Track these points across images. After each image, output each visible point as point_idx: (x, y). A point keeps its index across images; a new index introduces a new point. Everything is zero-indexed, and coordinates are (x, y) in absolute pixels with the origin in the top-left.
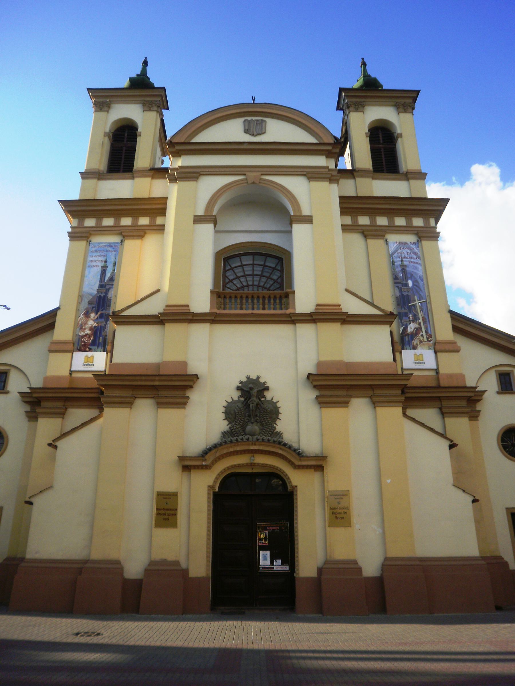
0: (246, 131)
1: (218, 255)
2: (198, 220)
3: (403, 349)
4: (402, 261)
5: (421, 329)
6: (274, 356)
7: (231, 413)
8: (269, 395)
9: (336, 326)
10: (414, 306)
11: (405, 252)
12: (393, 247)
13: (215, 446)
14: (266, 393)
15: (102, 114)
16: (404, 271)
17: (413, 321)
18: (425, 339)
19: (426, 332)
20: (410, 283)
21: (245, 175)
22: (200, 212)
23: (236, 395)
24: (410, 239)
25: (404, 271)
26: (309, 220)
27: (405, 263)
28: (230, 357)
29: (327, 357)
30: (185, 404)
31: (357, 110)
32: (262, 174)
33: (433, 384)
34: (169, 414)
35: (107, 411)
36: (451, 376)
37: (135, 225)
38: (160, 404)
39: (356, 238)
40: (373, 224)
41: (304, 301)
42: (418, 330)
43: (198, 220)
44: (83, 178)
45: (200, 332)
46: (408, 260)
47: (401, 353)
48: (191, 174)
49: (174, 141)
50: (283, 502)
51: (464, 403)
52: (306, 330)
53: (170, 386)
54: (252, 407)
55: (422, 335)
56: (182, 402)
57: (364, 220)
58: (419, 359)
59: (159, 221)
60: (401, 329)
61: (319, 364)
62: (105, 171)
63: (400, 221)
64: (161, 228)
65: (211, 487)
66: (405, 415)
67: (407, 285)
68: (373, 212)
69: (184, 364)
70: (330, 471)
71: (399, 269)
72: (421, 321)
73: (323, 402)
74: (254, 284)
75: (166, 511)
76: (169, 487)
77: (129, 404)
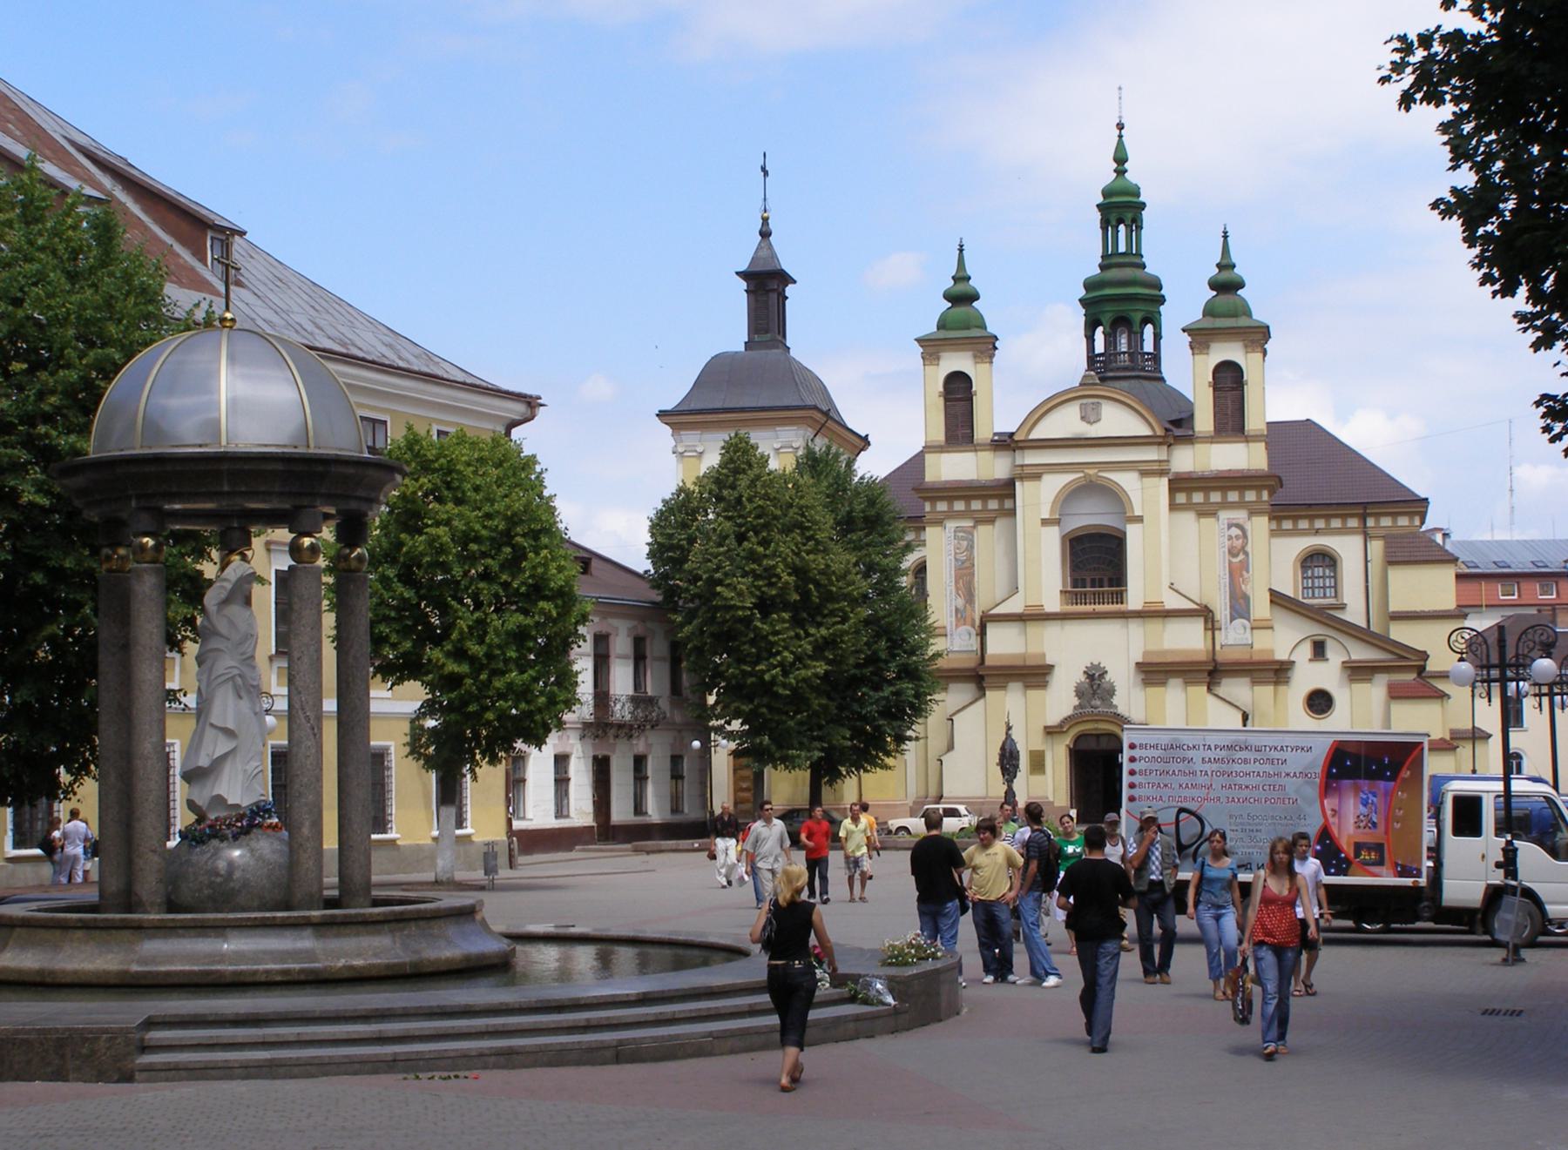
0: (1083, 418)
1: (1063, 538)
2: (1045, 522)
6: (1113, 647)
7: (1079, 693)
14: (1108, 677)
15: (930, 369)
23: (1083, 678)
26: (1140, 519)
29: (1152, 647)
34: (1032, 693)
36: (1262, 651)
37: (985, 510)
38: (1027, 687)
39: (1188, 518)
40: (1207, 502)
41: (1136, 596)
43: (1045, 522)
48: (1035, 474)
49: (1016, 438)
51: (1271, 674)
52: (1135, 628)
53: (1035, 675)
54: (1095, 684)
56: (1043, 685)
57: (1198, 497)
59: (1008, 504)
61: (1145, 653)
66: (1209, 690)
77: (1004, 687)
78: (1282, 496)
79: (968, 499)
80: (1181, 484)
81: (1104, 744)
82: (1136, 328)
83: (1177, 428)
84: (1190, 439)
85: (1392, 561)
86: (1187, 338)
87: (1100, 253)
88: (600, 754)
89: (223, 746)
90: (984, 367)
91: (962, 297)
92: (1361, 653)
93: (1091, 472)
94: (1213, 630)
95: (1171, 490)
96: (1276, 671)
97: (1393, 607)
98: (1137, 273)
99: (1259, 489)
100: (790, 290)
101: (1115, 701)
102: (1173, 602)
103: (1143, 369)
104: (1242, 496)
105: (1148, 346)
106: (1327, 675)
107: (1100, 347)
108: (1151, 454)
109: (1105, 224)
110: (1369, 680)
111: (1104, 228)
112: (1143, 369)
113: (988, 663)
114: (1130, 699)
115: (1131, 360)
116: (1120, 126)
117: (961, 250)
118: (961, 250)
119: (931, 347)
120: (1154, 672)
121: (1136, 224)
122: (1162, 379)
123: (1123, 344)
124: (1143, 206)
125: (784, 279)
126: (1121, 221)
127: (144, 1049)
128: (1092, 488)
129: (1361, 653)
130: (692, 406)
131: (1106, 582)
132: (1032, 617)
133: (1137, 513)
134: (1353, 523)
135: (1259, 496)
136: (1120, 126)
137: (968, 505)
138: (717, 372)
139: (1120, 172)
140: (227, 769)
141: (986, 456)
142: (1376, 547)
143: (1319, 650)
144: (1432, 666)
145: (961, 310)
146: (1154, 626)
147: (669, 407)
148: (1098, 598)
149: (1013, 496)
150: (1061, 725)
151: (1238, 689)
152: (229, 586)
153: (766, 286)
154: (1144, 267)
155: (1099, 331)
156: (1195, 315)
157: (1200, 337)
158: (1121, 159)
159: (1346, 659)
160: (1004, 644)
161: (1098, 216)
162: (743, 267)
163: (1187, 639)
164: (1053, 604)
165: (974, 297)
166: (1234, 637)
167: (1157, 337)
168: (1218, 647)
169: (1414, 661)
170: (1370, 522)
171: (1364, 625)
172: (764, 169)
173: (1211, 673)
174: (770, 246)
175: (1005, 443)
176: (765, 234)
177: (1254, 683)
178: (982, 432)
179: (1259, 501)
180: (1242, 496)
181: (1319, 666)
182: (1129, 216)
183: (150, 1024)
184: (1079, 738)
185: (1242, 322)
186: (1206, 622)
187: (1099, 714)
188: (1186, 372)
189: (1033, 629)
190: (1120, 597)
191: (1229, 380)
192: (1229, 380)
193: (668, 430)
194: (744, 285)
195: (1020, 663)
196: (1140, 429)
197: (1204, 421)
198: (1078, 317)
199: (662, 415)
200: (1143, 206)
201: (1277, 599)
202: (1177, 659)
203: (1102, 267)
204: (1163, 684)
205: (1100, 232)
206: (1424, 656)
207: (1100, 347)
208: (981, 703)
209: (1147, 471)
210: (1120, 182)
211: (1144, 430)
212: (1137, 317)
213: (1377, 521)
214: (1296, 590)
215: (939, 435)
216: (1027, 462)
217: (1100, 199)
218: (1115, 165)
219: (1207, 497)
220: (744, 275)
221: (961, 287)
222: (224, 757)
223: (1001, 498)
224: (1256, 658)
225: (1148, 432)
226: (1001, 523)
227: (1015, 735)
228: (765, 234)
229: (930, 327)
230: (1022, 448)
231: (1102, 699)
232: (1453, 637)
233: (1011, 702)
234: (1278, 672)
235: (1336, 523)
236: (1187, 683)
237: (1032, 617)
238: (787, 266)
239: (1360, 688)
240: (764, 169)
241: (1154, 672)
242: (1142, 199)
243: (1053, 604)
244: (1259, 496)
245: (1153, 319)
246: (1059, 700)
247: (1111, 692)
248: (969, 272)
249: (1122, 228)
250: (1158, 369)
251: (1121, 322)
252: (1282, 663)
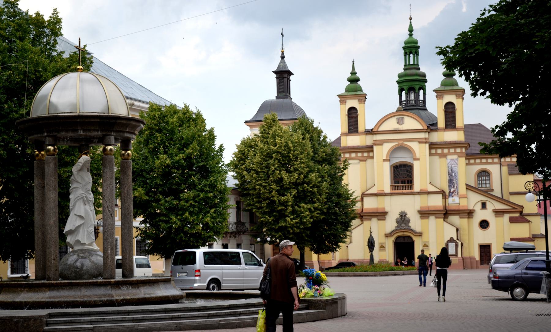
0: (398, 123)
1: (391, 166)
2: (384, 161)
6: (408, 204)
7: (397, 222)
8: (407, 216)
9: (426, 196)
11: (453, 162)
12: (449, 161)
13: (394, 231)
16: (451, 170)
20: (453, 174)
22: (385, 158)
23: (398, 216)
24: (455, 157)
25: (451, 170)
26: (418, 159)
28: (396, 205)
31: (440, 99)
33: (457, 208)
34: (381, 222)
35: (364, 222)
36: (463, 206)
37: (363, 156)
38: (378, 220)
39: (437, 158)
40: (443, 152)
41: (417, 187)
42: (454, 191)
43: (384, 161)
45: (387, 198)
48: (380, 143)
50: (411, 244)
51: (467, 214)
52: (417, 197)
53: (381, 215)
54: (403, 219)
56: (384, 219)
57: (439, 151)
58: (454, 200)
59: (371, 154)
61: (421, 207)
62: (347, 131)
63: (452, 150)
64: (372, 157)
66: (444, 220)
68: (442, 148)
69: (384, 208)
70: (424, 235)
71: (450, 169)
73: (422, 218)
74: (402, 176)
75: (382, 247)
77: (370, 220)
78: (470, 151)
79: (356, 152)
80: (432, 146)
81: (406, 240)
82: (417, 91)
83: (432, 127)
84: (436, 130)
85: (510, 174)
86: (435, 94)
87: (404, 64)
88: (225, 243)
89: (79, 222)
90: (362, 105)
91: (354, 80)
92: (500, 206)
93: (401, 142)
94: (445, 198)
95: (430, 149)
96: (468, 213)
97: (512, 190)
98: (417, 71)
99: (461, 147)
100: (292, 77)
101: (410, 224)
102: (431, 189)
103: (419, 106)
104: (455, 150)
105: (421, 98)
106: (487, 215)
107: (404, 98)
108: (422, 135)
109: (405, 54)
110: (503, 216)
111: (405, 55)
112: (419, 106)
113: (364, 211)
114: (416, 223)
115: (415, 103)
116: (411, 19)
117: (353, 63)
118: (353, 63)
119: (343, 98)
120: (425, 214)
121: (416, 53)
122: (426, 110)
123: (412, 96)
124: (419, 47)
125: (290, 73)
126: (411, 53)
127: (48, 324)
128: (401, 148)
129: (500, 206)
130: (257, 119)
131: (406, 181)
132: (380, 194)
133: (418, 157)
134: (496, 160)
135: (462, 150)
136: (411, 19)
137: (357, 155)
138: (265, 107)
139: (411, 35)
140: (81, 230)
141: (364, 137)
142: (505, 169)
143: (484, 206)
144: (525, 211)
145: (354, 85)
146: (425, 196)
147: (249, 119)
148: (404, 188)
149: (373, 151)
150: (391, 233)
151: (454, 219)
152: (81, 164)
153: (283, 76)
154: (419, 69)
155: (404, 93)
156: (438, 85)
157: (439, 93)
158: (411, 30)
159: (494, 208)
160: (370, 204)
161: (403, 51)
162: (275, 69)
163: (436, 202)
164: (388, 190)
165: (358, 80)
166: (453, 201)
167: (425, 94)
168: (447, 205)
169: (519, 209)
170: (502, 160)
171: (501, 197)
172: (283, 35)
173: (445, 214)
174: (284, 62)
175: (369, 132)
176: (283, 57)
177: (460, 218)
178: (361, 129)
179: (462, 152)
180: (455, 150)
181: (484, 211)
182: (414, 51)
183: (51, 315)
184: (398, 238)
185: (455, 88)
186: (443, 196)
187: (404, 229)
188: (435, 107)
189: (380, 198)
190: (411, 187)
191: (450, 109)
192: (450, 109)
193: (248, 128)
194: (275, 76)
195: (375, 211)
196: (419, 127)
197: (441, 123)
198: (396, 87)
199: (246, 122)
200: (419, 47)
201: (468, 187)
202: (433, 209)
203: (405, 69)
204: (428, 218)
205: (404, 57)
206: (522, 207)
207: (404, 98)
208: (362, 226)
209: (421, 141)
210: (411, 39)
211: (421, 127)
212: (417, 87)
213: (505, 160)
214: (475, 184)
215: (346, 130)
216: (378, 139)
217: (404, 45)
218: (409, 33)
219: (443, 151)
220: (275, 72)
221: (353, 77)
222: (79, 226)
223: (368, 152)
224: (461, 208)
225: (421, 128)
226: (369, 161)
227: (373, 235)
228: (283, 57)
229: (342, 91)
230: (376, 134)
231: (405, 224)
232: (526, 185)
233: (374, 224)
234: (470, 213)
235: (490, 160)
236: (436, 218)
237: (380, 194)
238: (291, 69)
239: (500, 219)
240: (283, 35)
241: (425, 214)
242: (419, 45)
243: (388, 190)
244: (462, 150)
245: (423, 88)
246: (390, 224)
247: (409, 221)
248: (356, 71)
249: (411, 55)
250: (425, 106)
251: (411, 89)
252: (470, 210)
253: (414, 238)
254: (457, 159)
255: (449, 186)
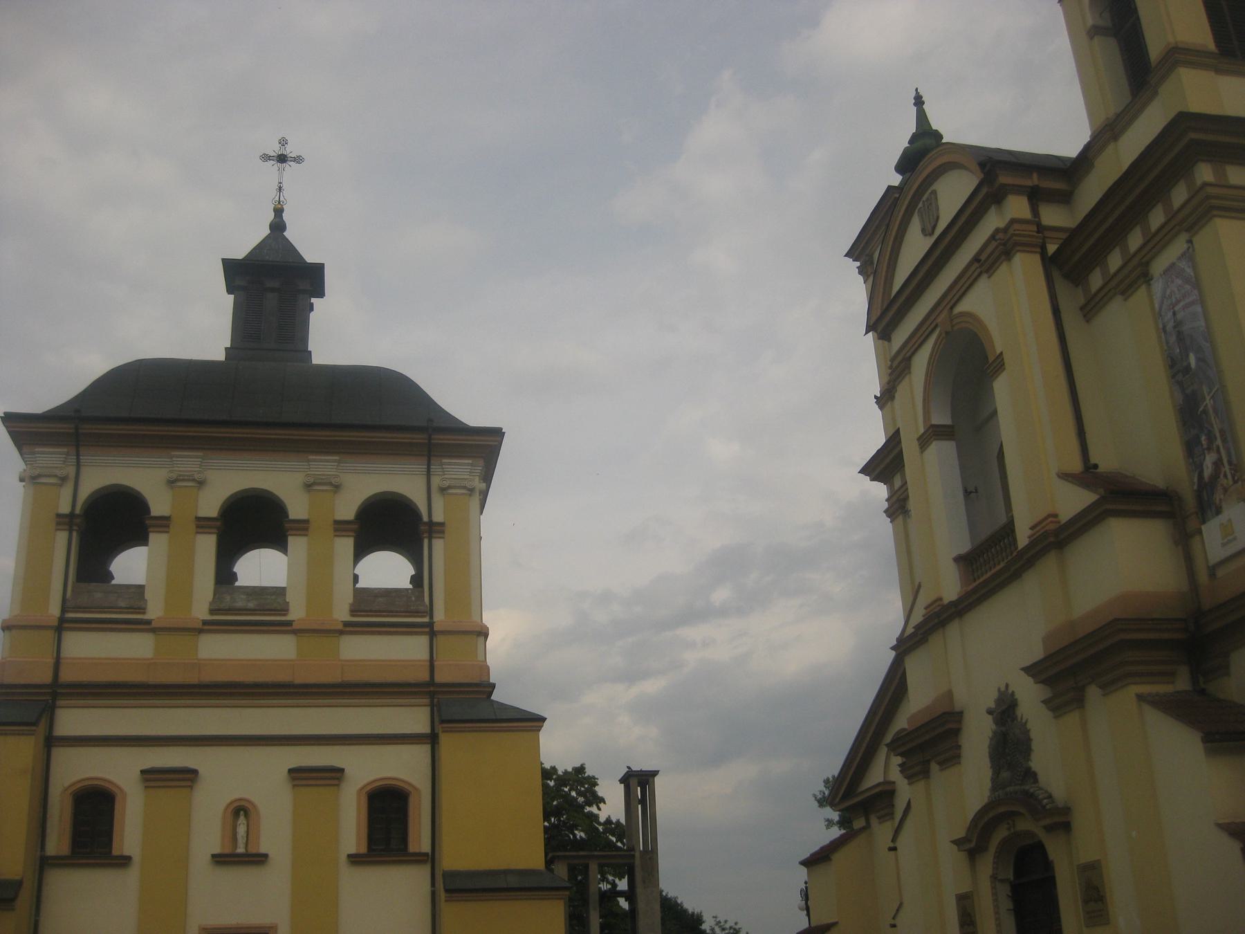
2: (924, 442)
3: (1204, 522)
4: (1174, 314)
5: (1220, 459)
10: (1205, 412)
16: (1180, 337)
17: (1209, 449)
18: (1231, 482)
19: (1230, 463)
21: (936, 326)
25: (1180, 337)
27: (1179, 316)
30: (959, 756)
32: (952, 308)
42: (1218, 464)
44: (881, 408)
46: (1182, 304)
47: (1200, 532)
55: (1225, 476)
57: (1115, 261)
60: (1196, 480)
65: (994, 878)
67: (1188, 368)
71: (1173, 339)
72: (1219, 442)
76: (964, 889)
99: (1180, 168)
168: (1203, 577)
253: (1055, 849)
254: (1189, 255)
255: (1191, 448)
